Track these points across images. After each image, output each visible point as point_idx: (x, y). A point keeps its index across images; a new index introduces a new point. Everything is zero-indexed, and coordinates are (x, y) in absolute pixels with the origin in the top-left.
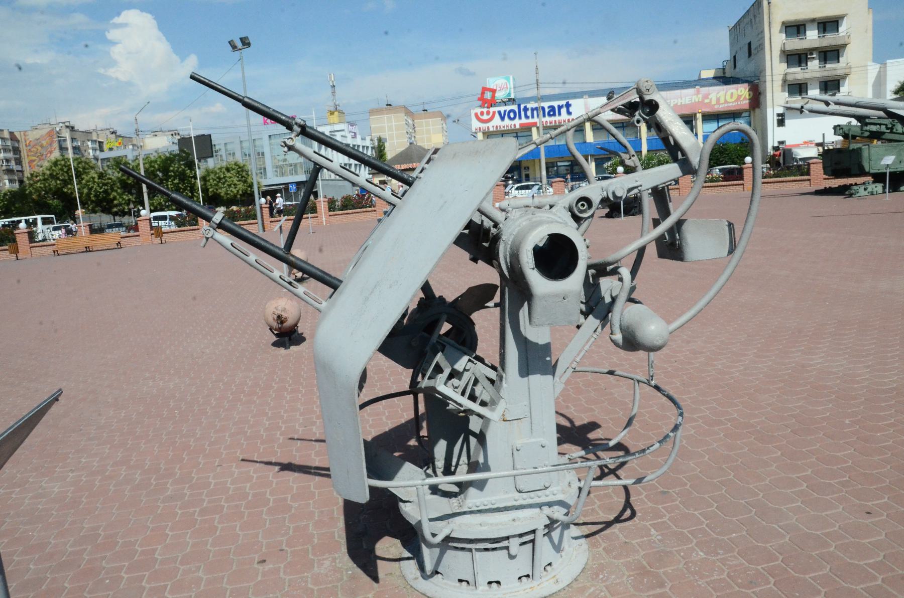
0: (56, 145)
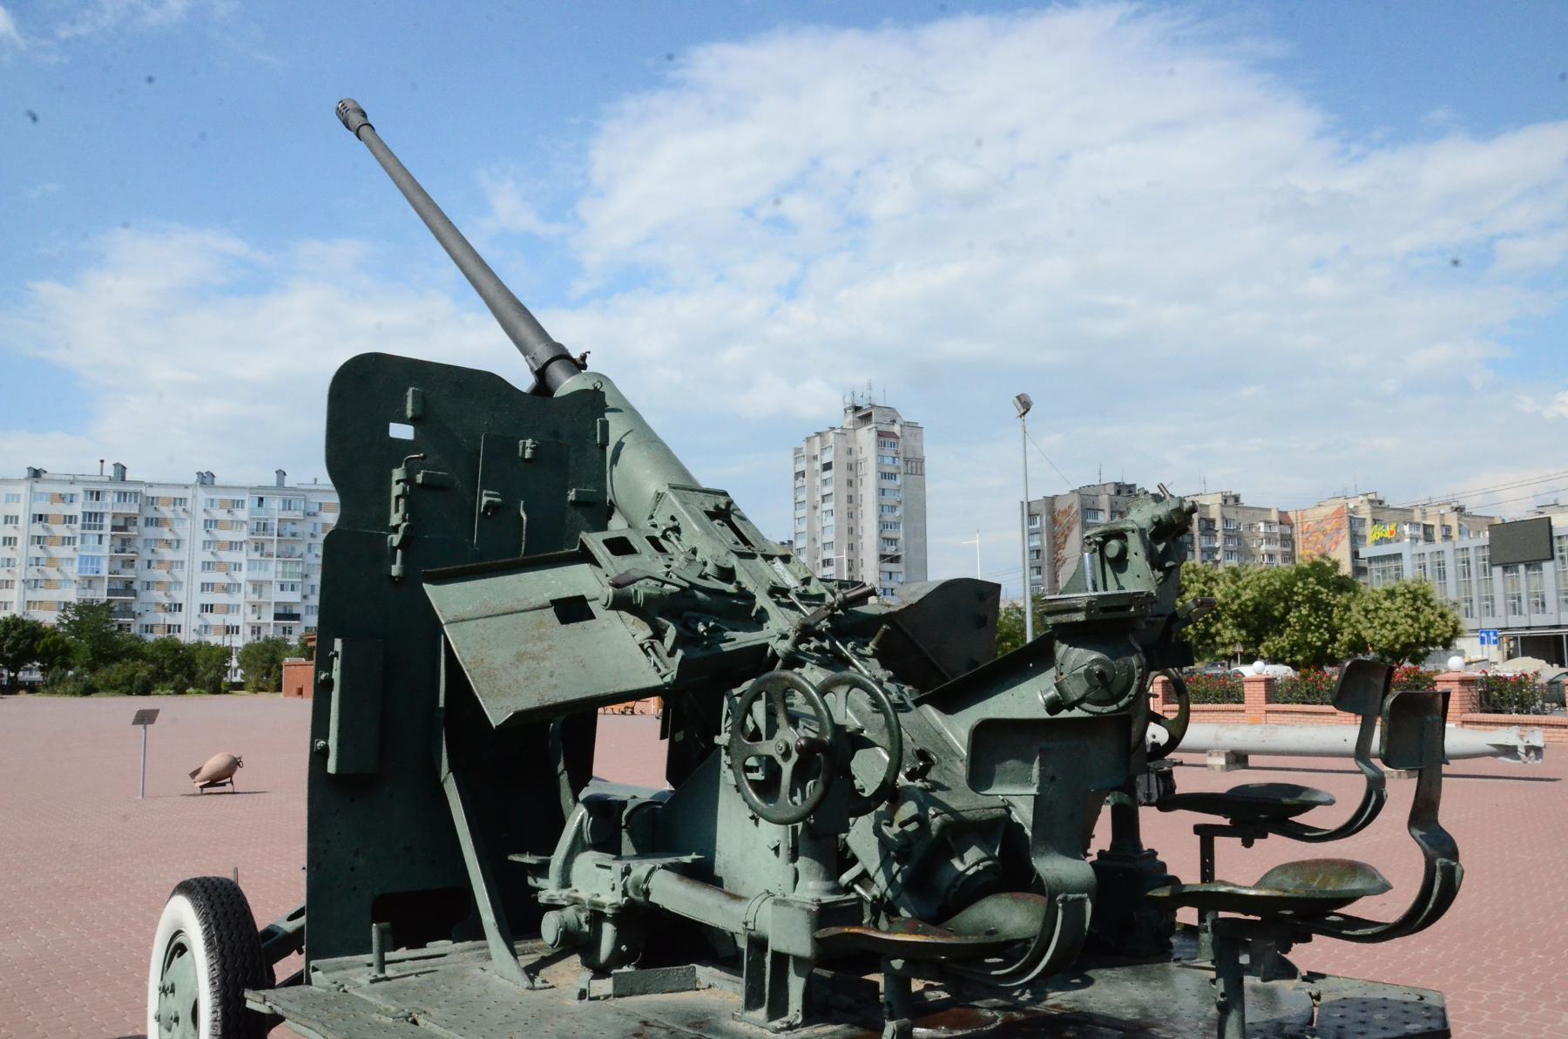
0: (1345, 532)
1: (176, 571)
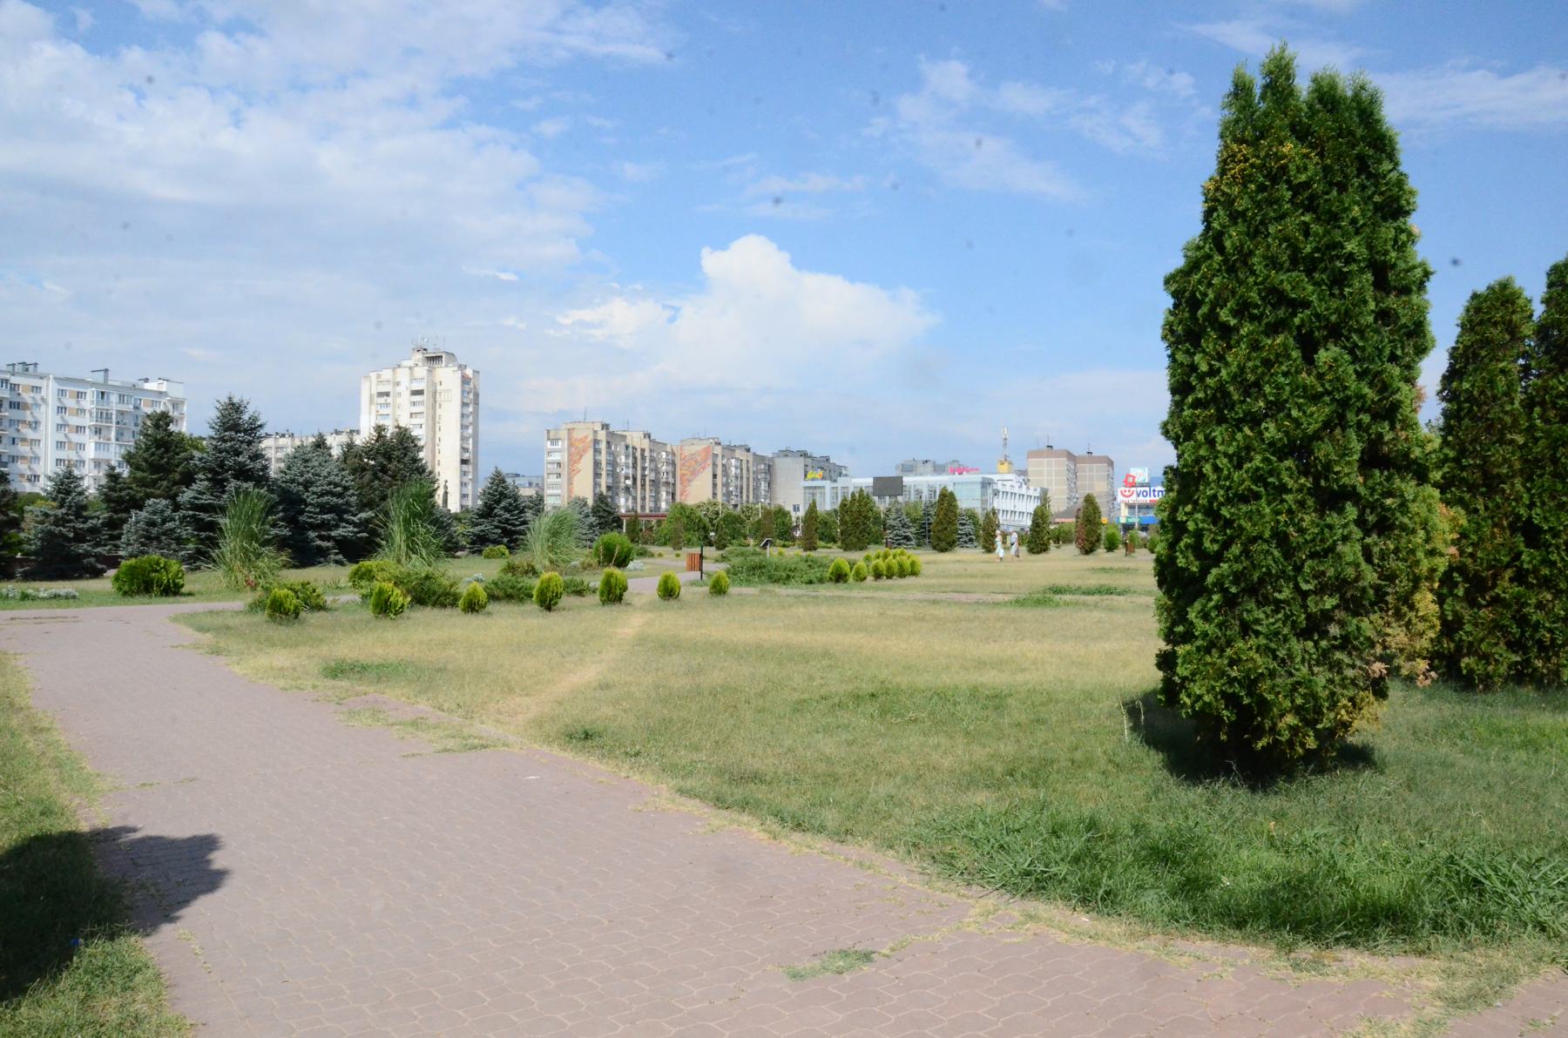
0: (710, 462)
1: (35, 449)
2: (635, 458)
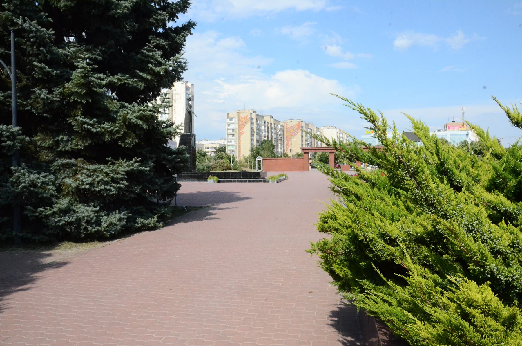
2: (268, 128)
